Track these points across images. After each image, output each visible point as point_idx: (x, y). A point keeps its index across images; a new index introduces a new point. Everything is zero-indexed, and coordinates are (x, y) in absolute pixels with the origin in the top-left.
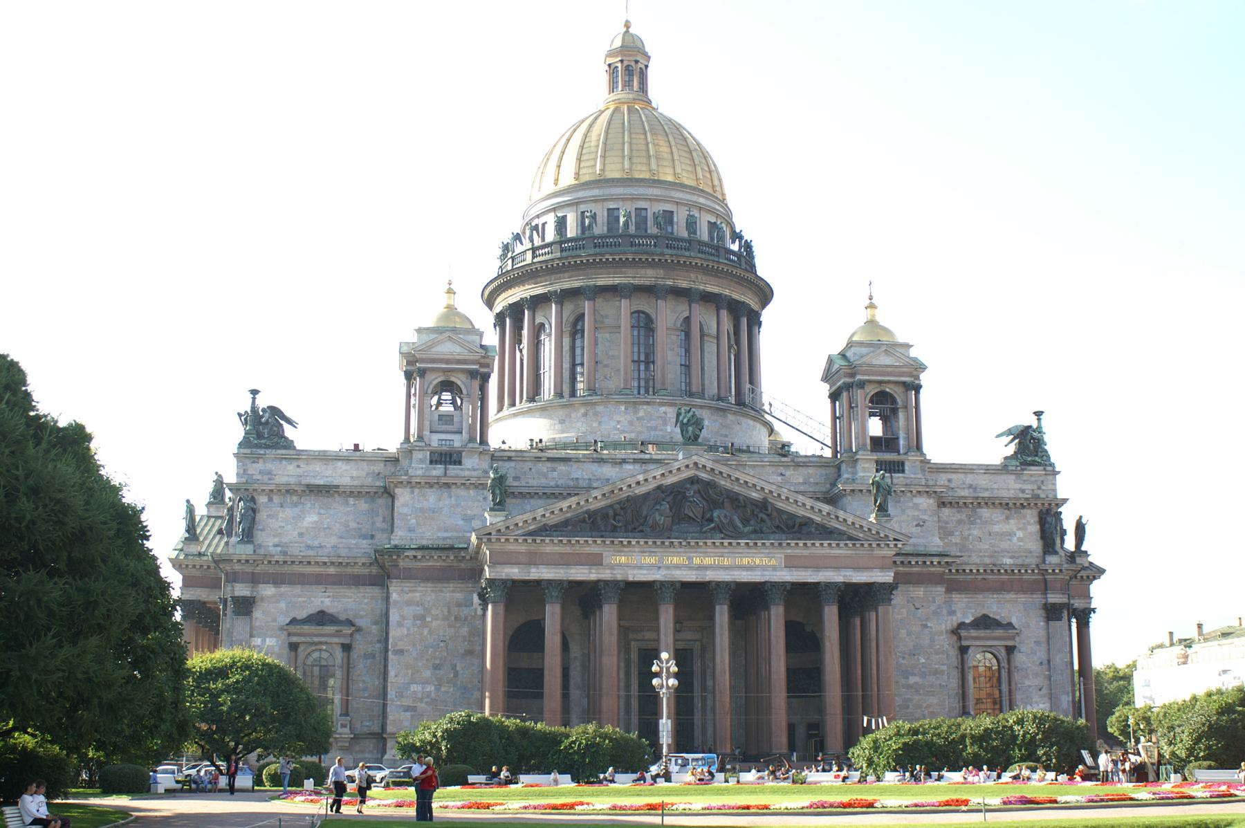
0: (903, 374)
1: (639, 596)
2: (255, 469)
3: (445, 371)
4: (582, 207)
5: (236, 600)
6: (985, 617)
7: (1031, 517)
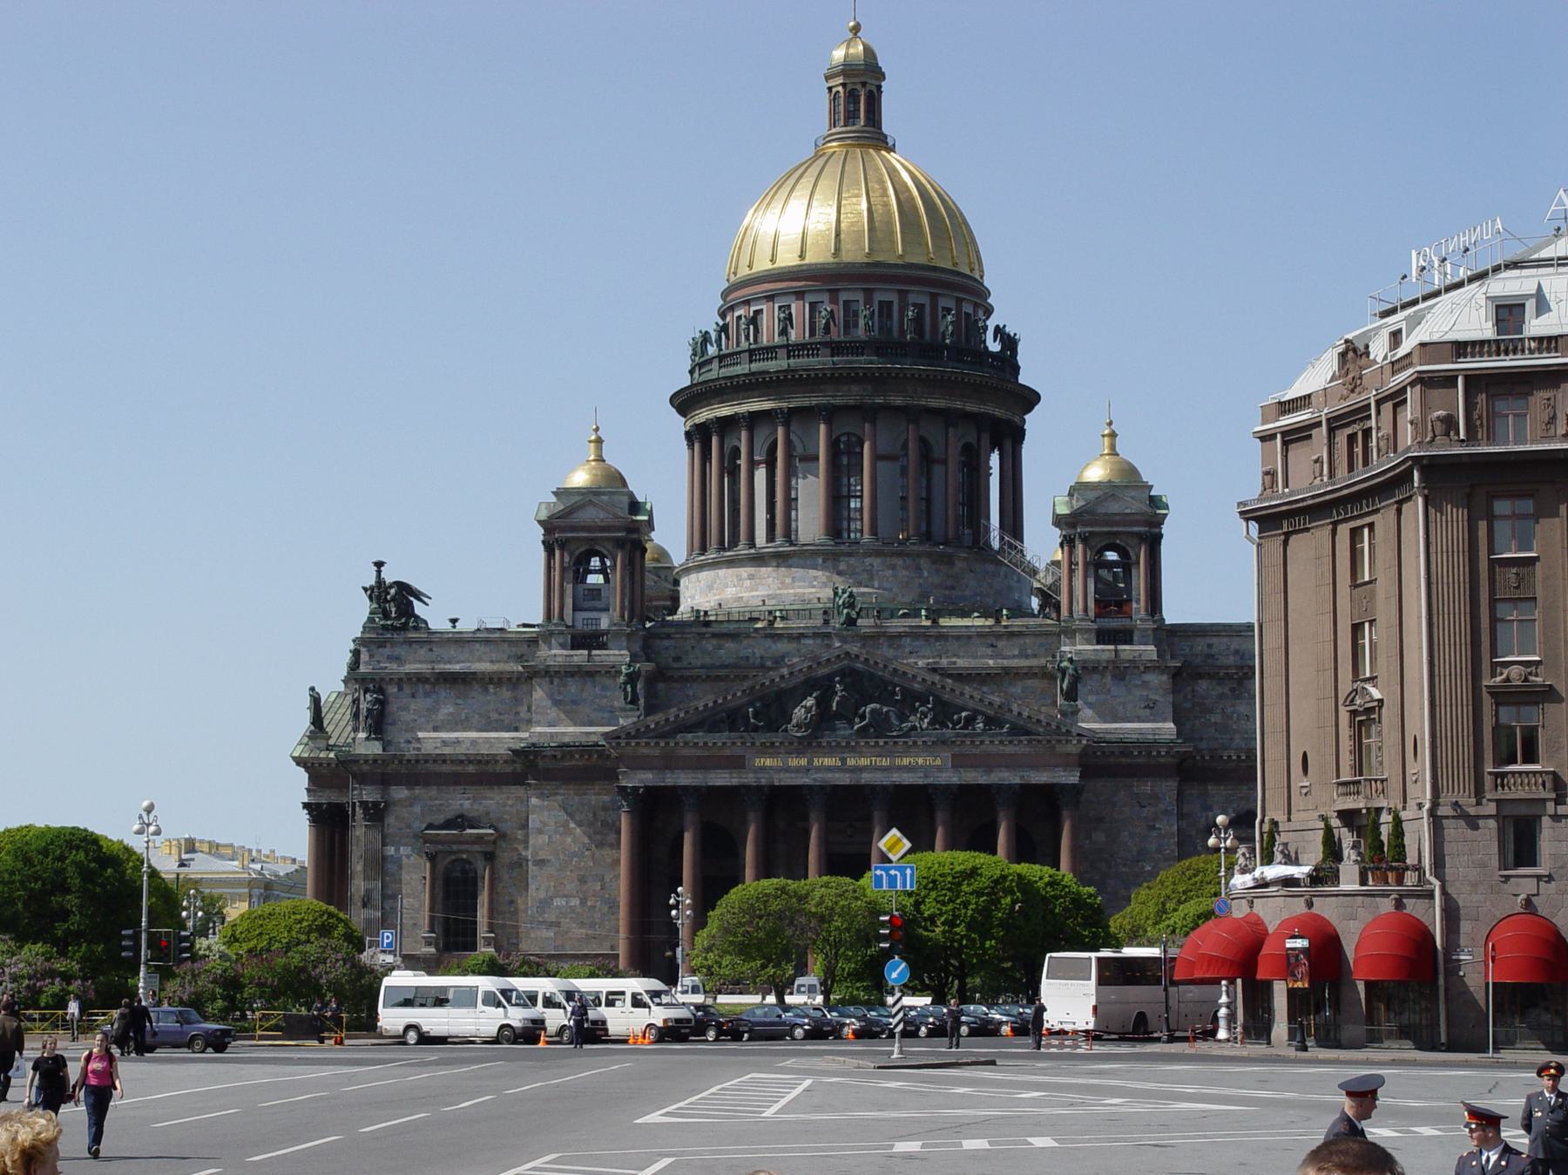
0: (1137, 523)
5: (364, 804)
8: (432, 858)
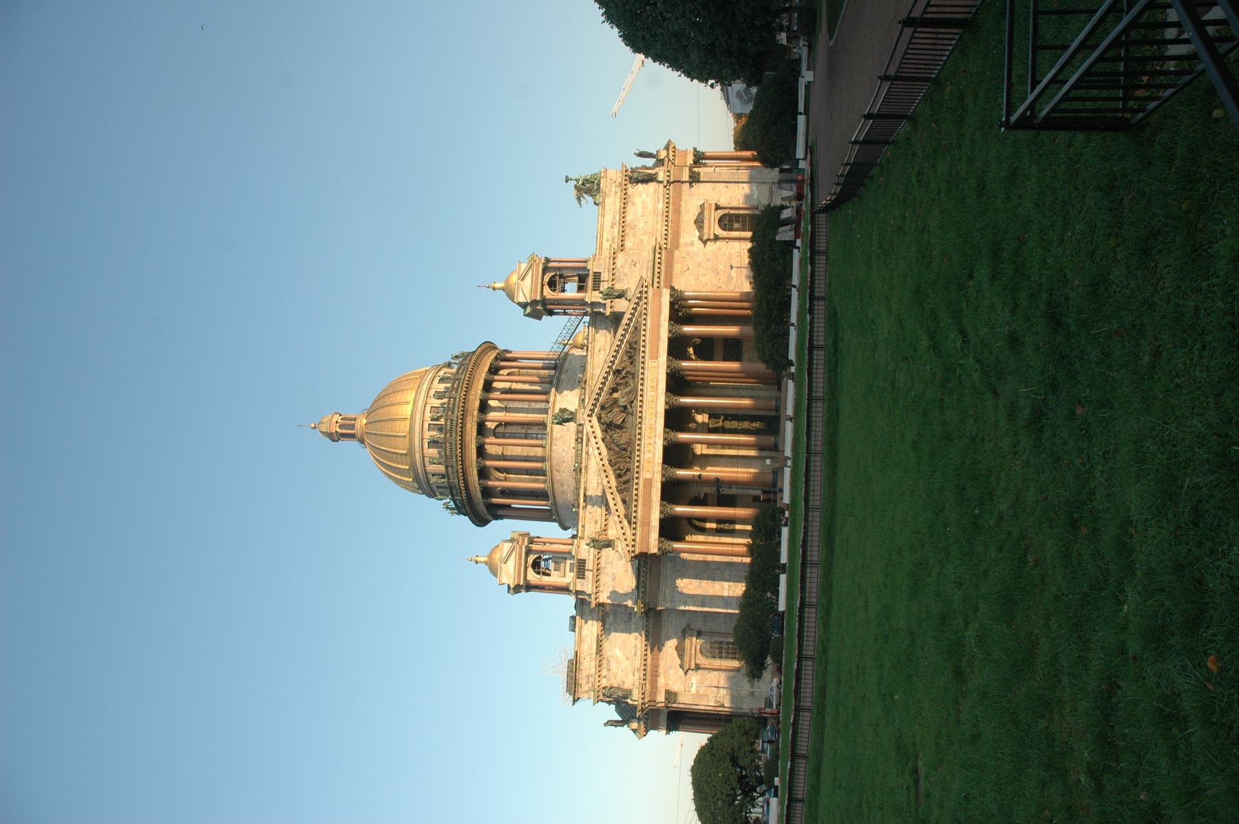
1: (675, 455)
2: (584, 685)
3: (526, 568)
4: (427, 464)
6: (696, 222)
7: (631, 189)
8: (698, 668)
